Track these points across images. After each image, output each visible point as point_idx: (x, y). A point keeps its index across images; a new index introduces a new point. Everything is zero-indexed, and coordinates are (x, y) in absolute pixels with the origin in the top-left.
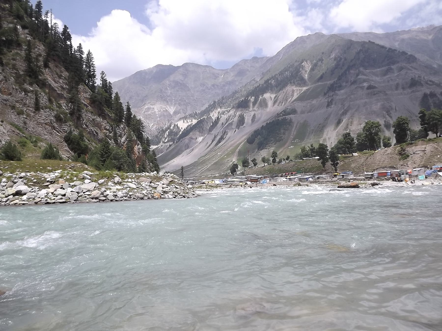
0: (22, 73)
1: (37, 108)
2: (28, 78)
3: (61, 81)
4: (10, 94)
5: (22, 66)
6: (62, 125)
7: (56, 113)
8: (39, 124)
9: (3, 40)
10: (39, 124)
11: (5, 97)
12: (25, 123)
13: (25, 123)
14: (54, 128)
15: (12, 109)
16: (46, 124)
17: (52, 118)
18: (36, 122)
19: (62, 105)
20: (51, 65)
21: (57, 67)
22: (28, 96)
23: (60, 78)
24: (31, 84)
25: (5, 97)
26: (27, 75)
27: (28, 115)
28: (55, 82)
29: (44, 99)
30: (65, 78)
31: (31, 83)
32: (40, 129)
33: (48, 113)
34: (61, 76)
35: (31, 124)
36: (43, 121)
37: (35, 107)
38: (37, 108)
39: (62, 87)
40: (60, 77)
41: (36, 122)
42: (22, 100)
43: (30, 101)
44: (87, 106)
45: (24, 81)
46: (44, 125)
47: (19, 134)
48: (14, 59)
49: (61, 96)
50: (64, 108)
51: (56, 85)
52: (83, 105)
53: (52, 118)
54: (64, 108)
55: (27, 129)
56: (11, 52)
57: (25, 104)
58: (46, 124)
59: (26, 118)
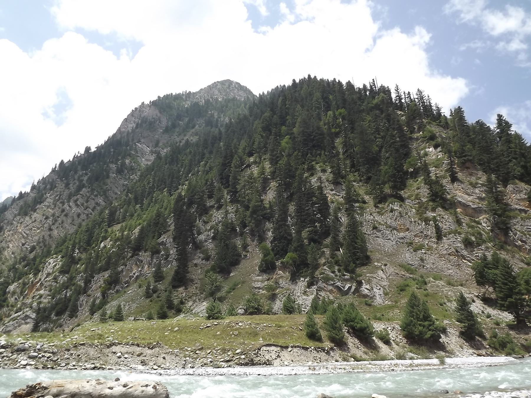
0: (424, 200)
1: (439, 236)
2: (431, 203)
3: (477, 191)
4: (408, 229)
5: (425, 192)
6: (474, 251)
7: (463, 236)
8: (441, 256)
9: (412, 172)
10: (441, 256)
11: (402, 234)
12: (422, 260)
13: (422, 260)
14: (463, 257)
15: (408, 247)
16: (449, 254)
17: (459, 245)
18: (438, 255)
19: (482, 221)
20: (460, 175)
21: (471, 175)
22: (429, 225)
23: (475, 188)
24: (433, 210)
25: (402, 234)
26: (430, 200)
27: (430, 249)
28: (469, 195)
29: (447, 223)
30: (483, 185)
31: (434, 208)
32: (442, 264)
33: (452, 240)
34: (477, 183)
35: (431, 260)
36: (445, 252)
37: (437, 236)
38: (439, 236)
39: (481, 199)
40: (474, 186)
41: (438, 255)
42: (422, 232)
43: (431, 231)
44: (526, 212)
45: (426, 209)
46: (447, 256)
47: (404, 275)
48: (418, 188)
49: (478, 211)
50: (484, 225)
51: (470, 198)
52: (517, 212)
53: (459, 245)
54: (484, 225)
55: (424, 266)
56: (418, 180)
57: (426, 236)
58: (449, 254)
59: (425, 253)
